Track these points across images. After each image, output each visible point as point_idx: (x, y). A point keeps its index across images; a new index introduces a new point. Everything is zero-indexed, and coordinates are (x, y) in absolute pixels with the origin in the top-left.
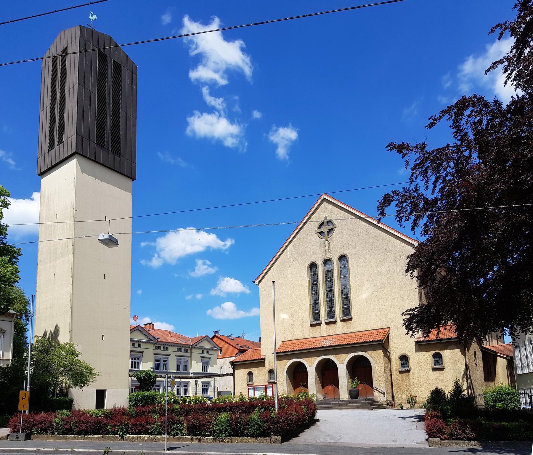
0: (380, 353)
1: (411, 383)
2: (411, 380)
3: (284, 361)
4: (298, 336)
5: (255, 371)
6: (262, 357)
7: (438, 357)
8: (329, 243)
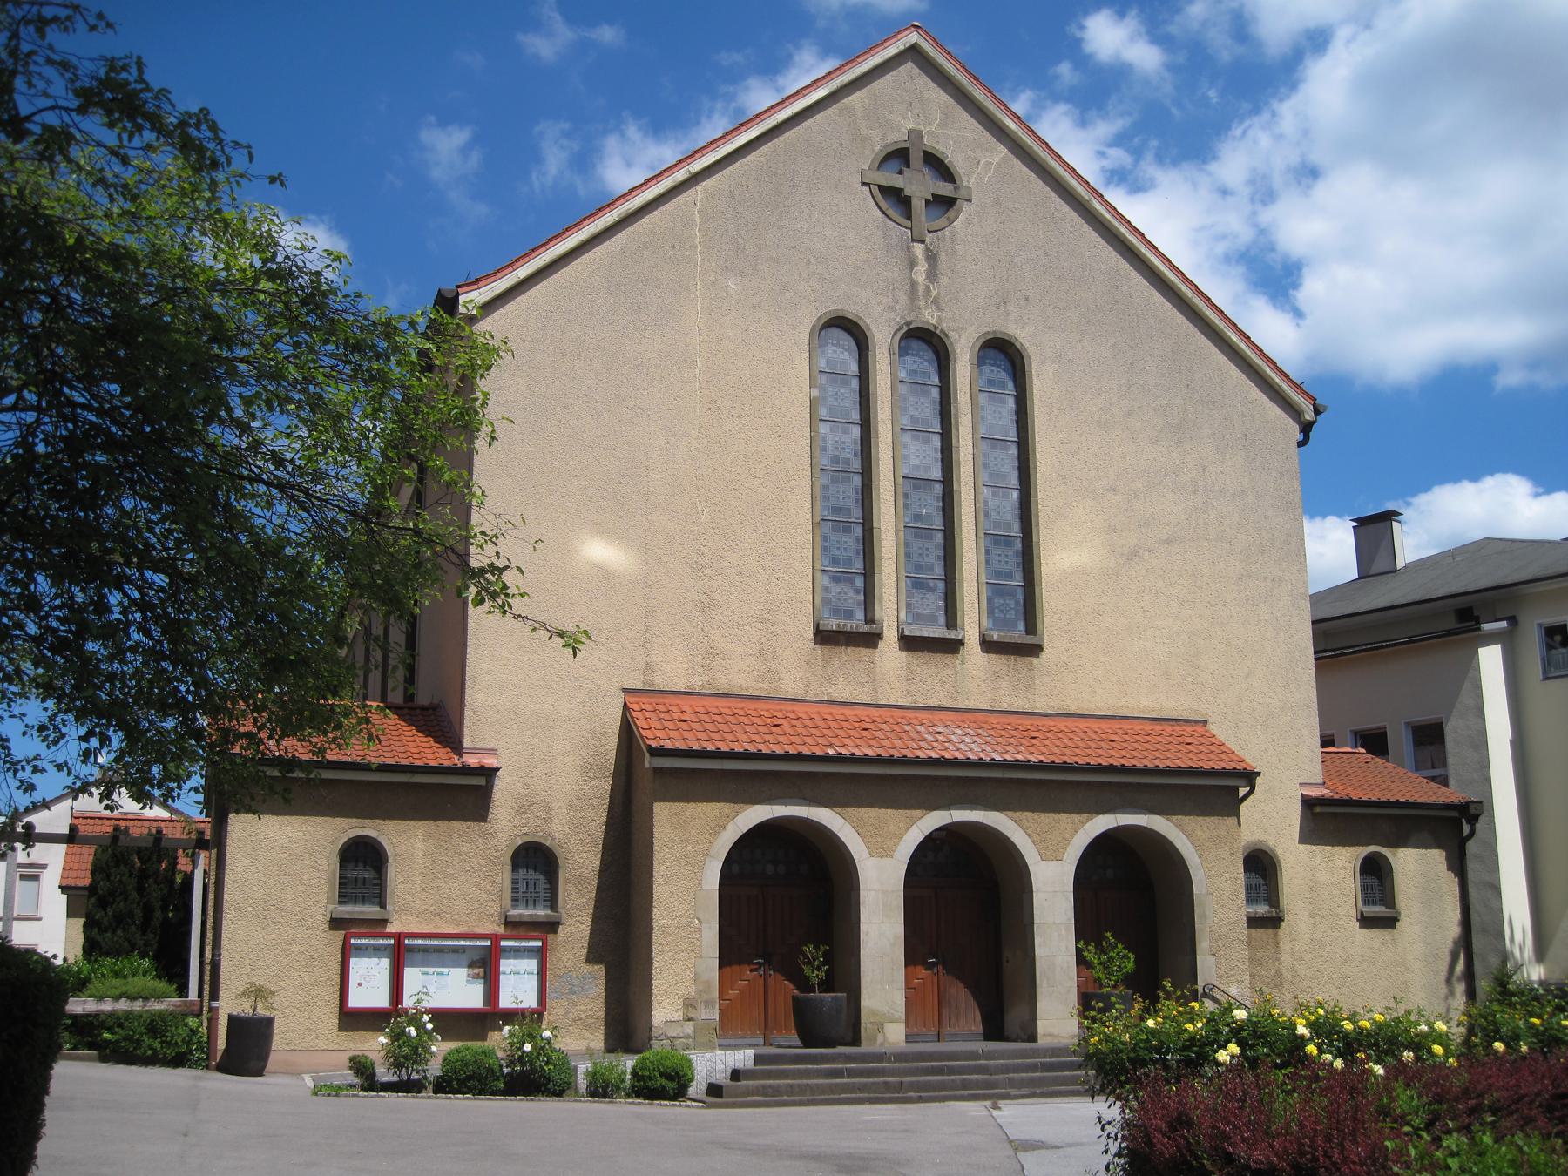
0: (1436, 858)
1: (1287, 974)
2: (1286, 959)
3: (712, 809)
4: (739, 675)
5: (409, 845)
6: (472, 760)
7: (1375, 875)
8: (932, 258)
